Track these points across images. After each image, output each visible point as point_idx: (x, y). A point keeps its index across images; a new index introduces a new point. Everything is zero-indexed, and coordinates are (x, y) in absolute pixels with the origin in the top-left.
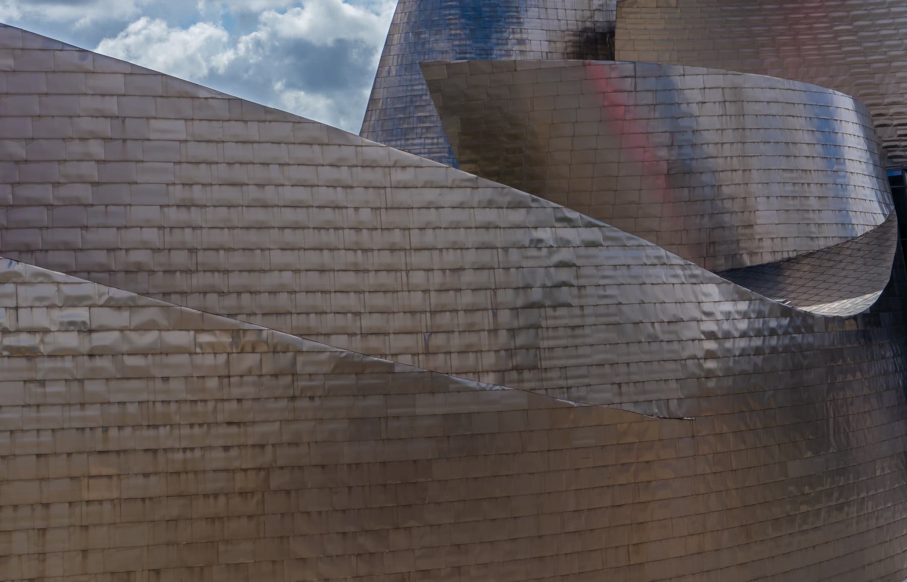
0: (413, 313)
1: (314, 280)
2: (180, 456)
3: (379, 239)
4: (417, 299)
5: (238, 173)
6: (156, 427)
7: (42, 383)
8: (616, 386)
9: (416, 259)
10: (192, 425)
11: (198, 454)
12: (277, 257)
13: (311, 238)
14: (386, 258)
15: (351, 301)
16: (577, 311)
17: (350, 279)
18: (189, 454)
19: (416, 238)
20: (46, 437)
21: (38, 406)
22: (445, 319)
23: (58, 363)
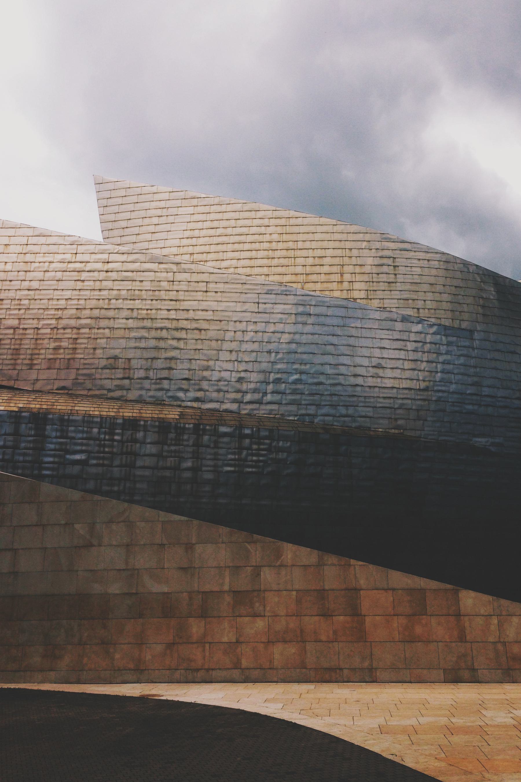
0: (296, 274)
1: (247, 263)
2: (145, 312)
3: (281, 245)
4: (299, 269)
5: (215, 224)
6: (134, 300)
7: (83, 281)
8: (416, 310)
9: (299, 253)
10: (152, 300)
11: (154, 311)
12: (230, 255)
13: (247, 246)
14: (284, 253)
15: (265, 270)
16: (393, 276)
17: (265, 262)
18: (149, 312)
19: (300, 245)
20: (82, 302)
21: (80, 290)
22: (314, 278)
23: (91, 274)
